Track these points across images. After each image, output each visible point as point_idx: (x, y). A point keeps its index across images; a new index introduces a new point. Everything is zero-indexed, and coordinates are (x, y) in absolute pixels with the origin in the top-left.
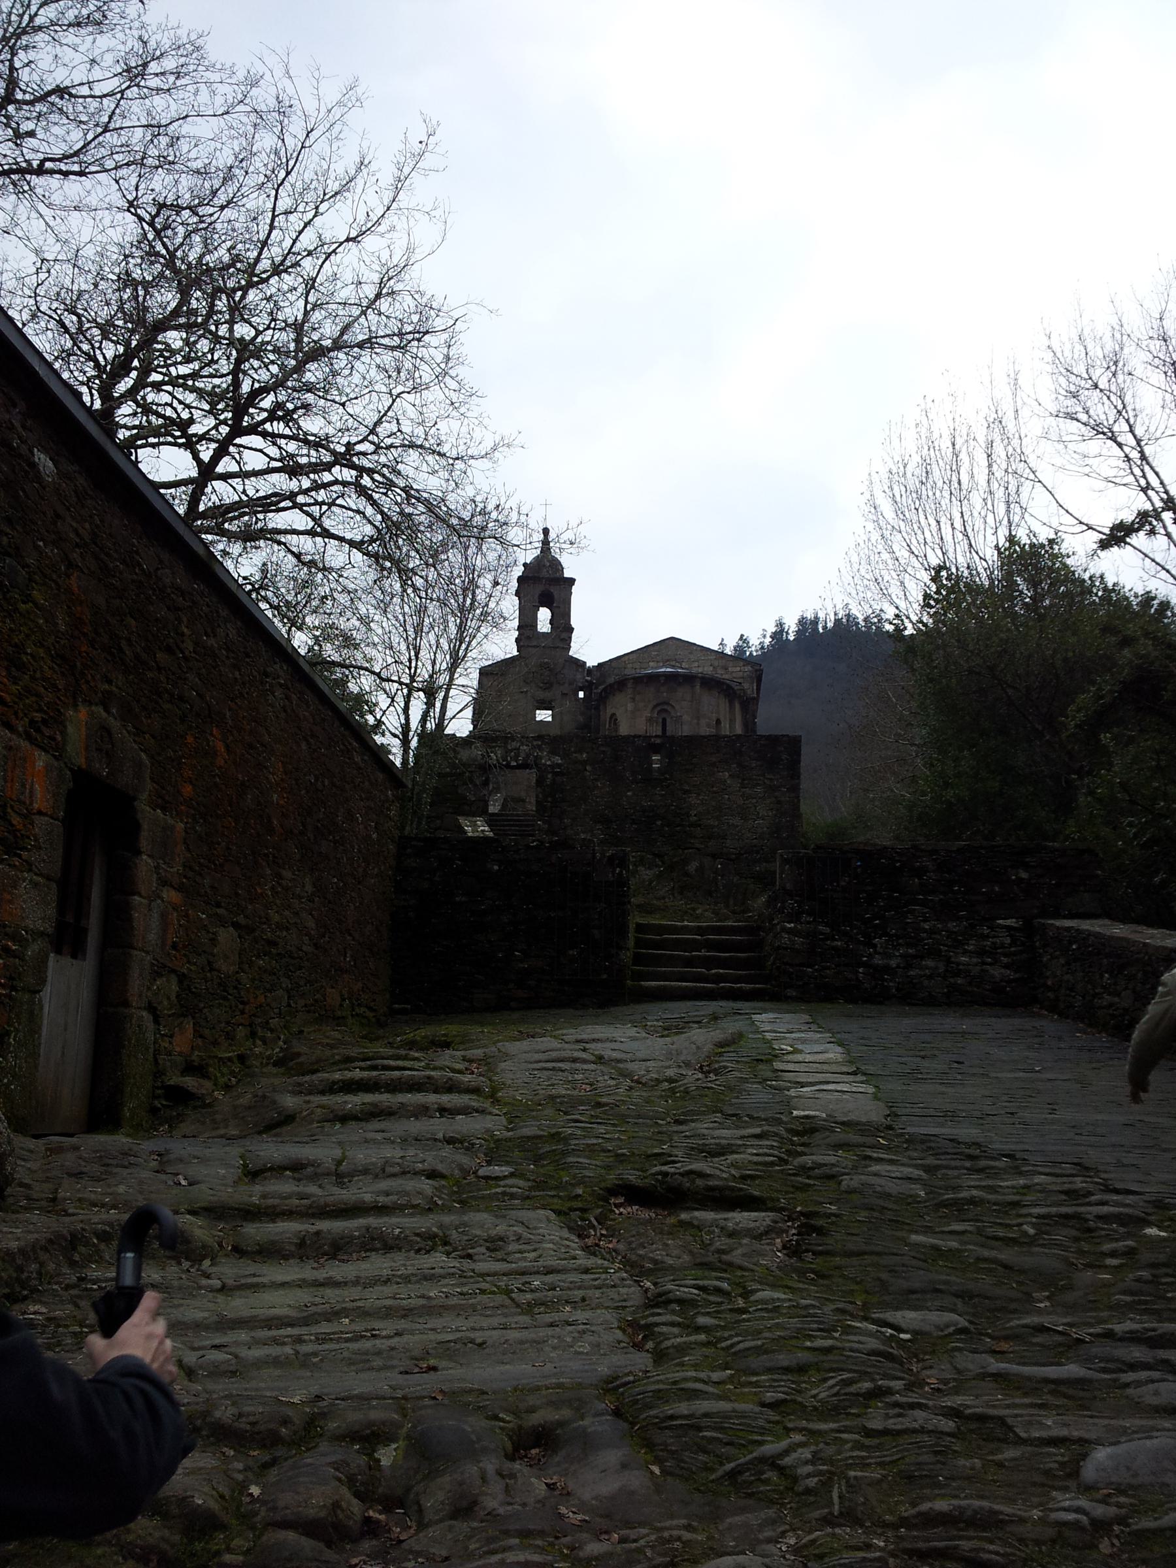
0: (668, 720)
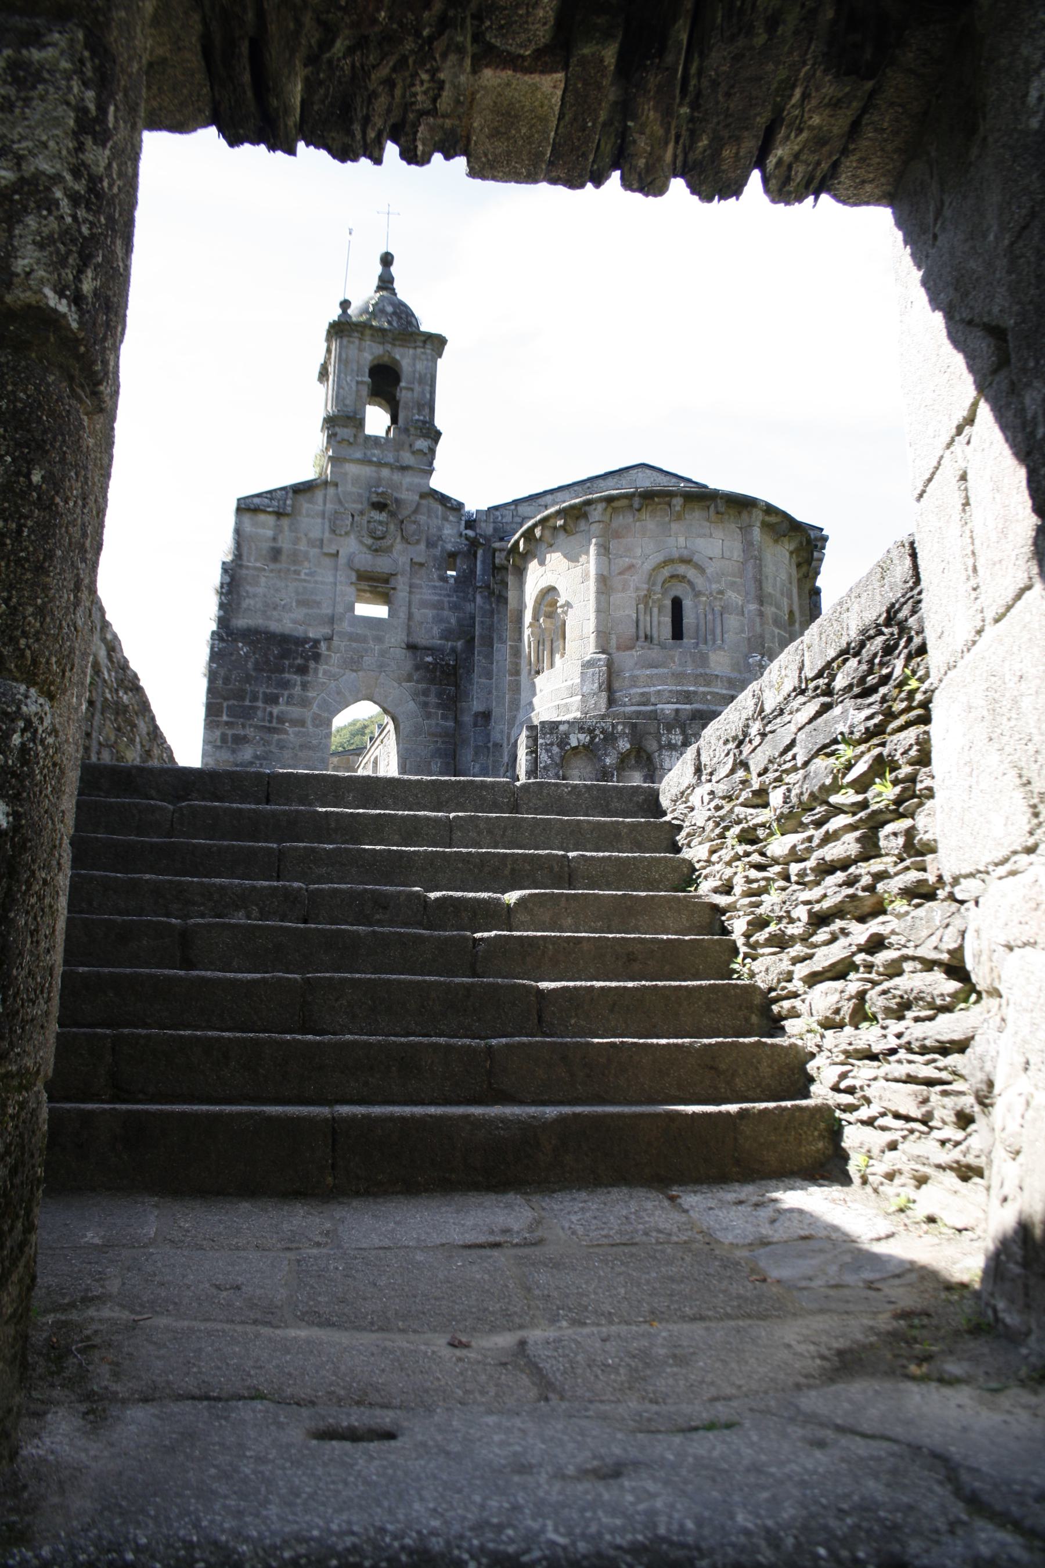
0: (687, 604)
